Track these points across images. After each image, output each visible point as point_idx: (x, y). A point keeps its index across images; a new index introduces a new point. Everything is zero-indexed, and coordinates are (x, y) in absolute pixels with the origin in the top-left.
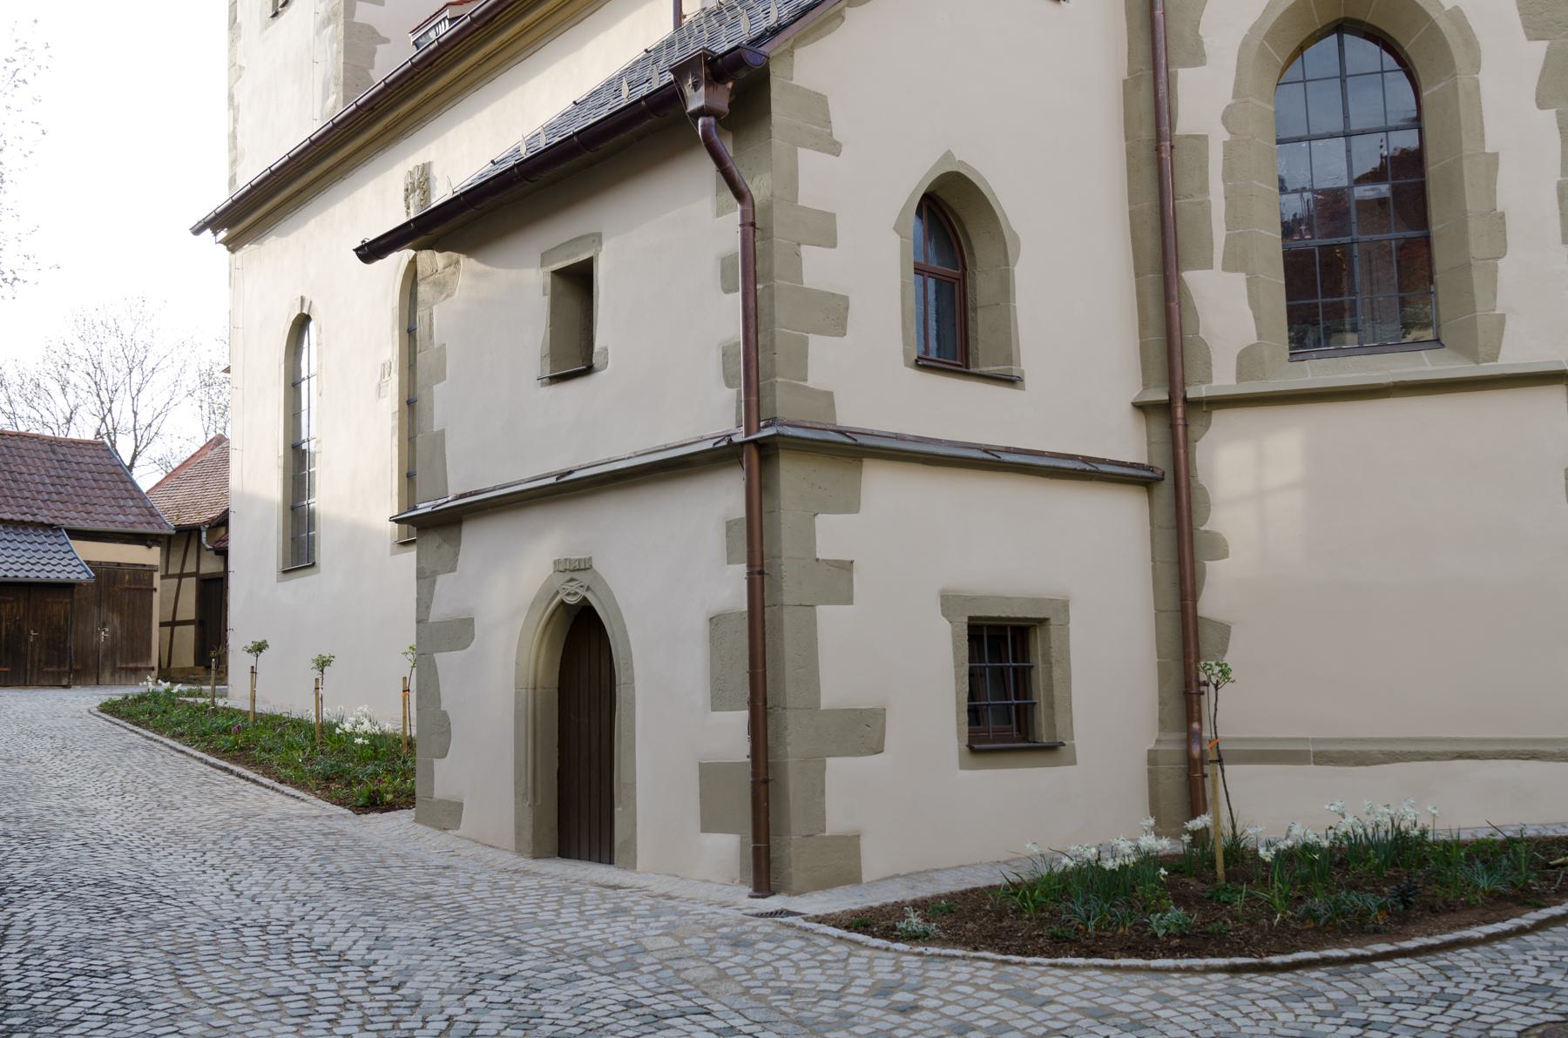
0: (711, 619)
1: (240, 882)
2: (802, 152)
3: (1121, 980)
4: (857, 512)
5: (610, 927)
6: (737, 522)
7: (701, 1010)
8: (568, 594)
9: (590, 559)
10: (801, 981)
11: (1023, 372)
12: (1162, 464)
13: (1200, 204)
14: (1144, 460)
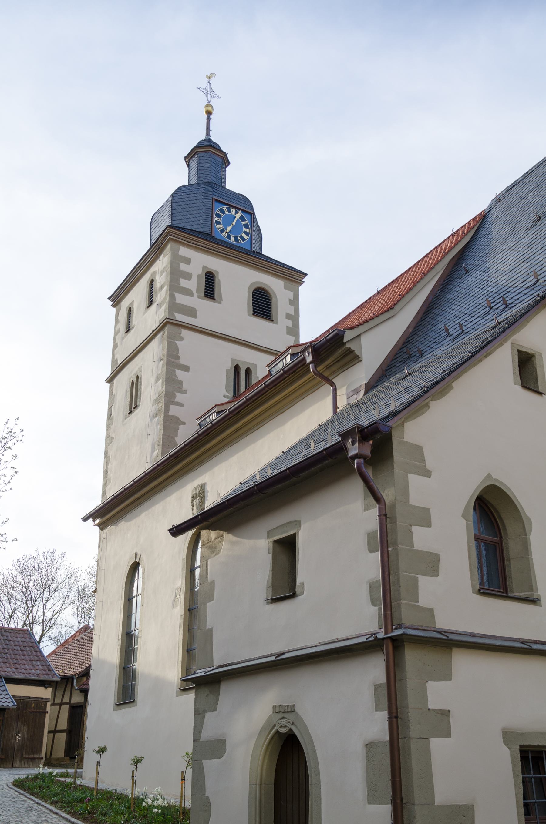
0: (366, 745)
2: (410, 476)
6: (380, 685)
8: (281, 727)
9: (294, 705)
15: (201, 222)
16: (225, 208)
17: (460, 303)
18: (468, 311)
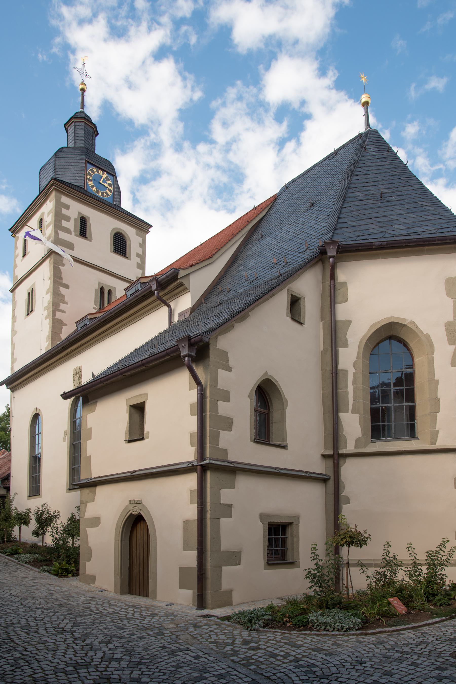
0: (184, 522)
1: (24, 602)
3: (323, 638)
4: (234, 488)
5: (152, 620)
6: (194, 491)
7: (187, 649)
8: (134, 511)
9: (142, 500)
10: (219, 639)
11: (287, 444)
12: (331, 474)
13: (345, 392)
14: (324, 473)
15: (77, 178)
16: (95, 169)
17: (256, 259)
18: (261, 264)
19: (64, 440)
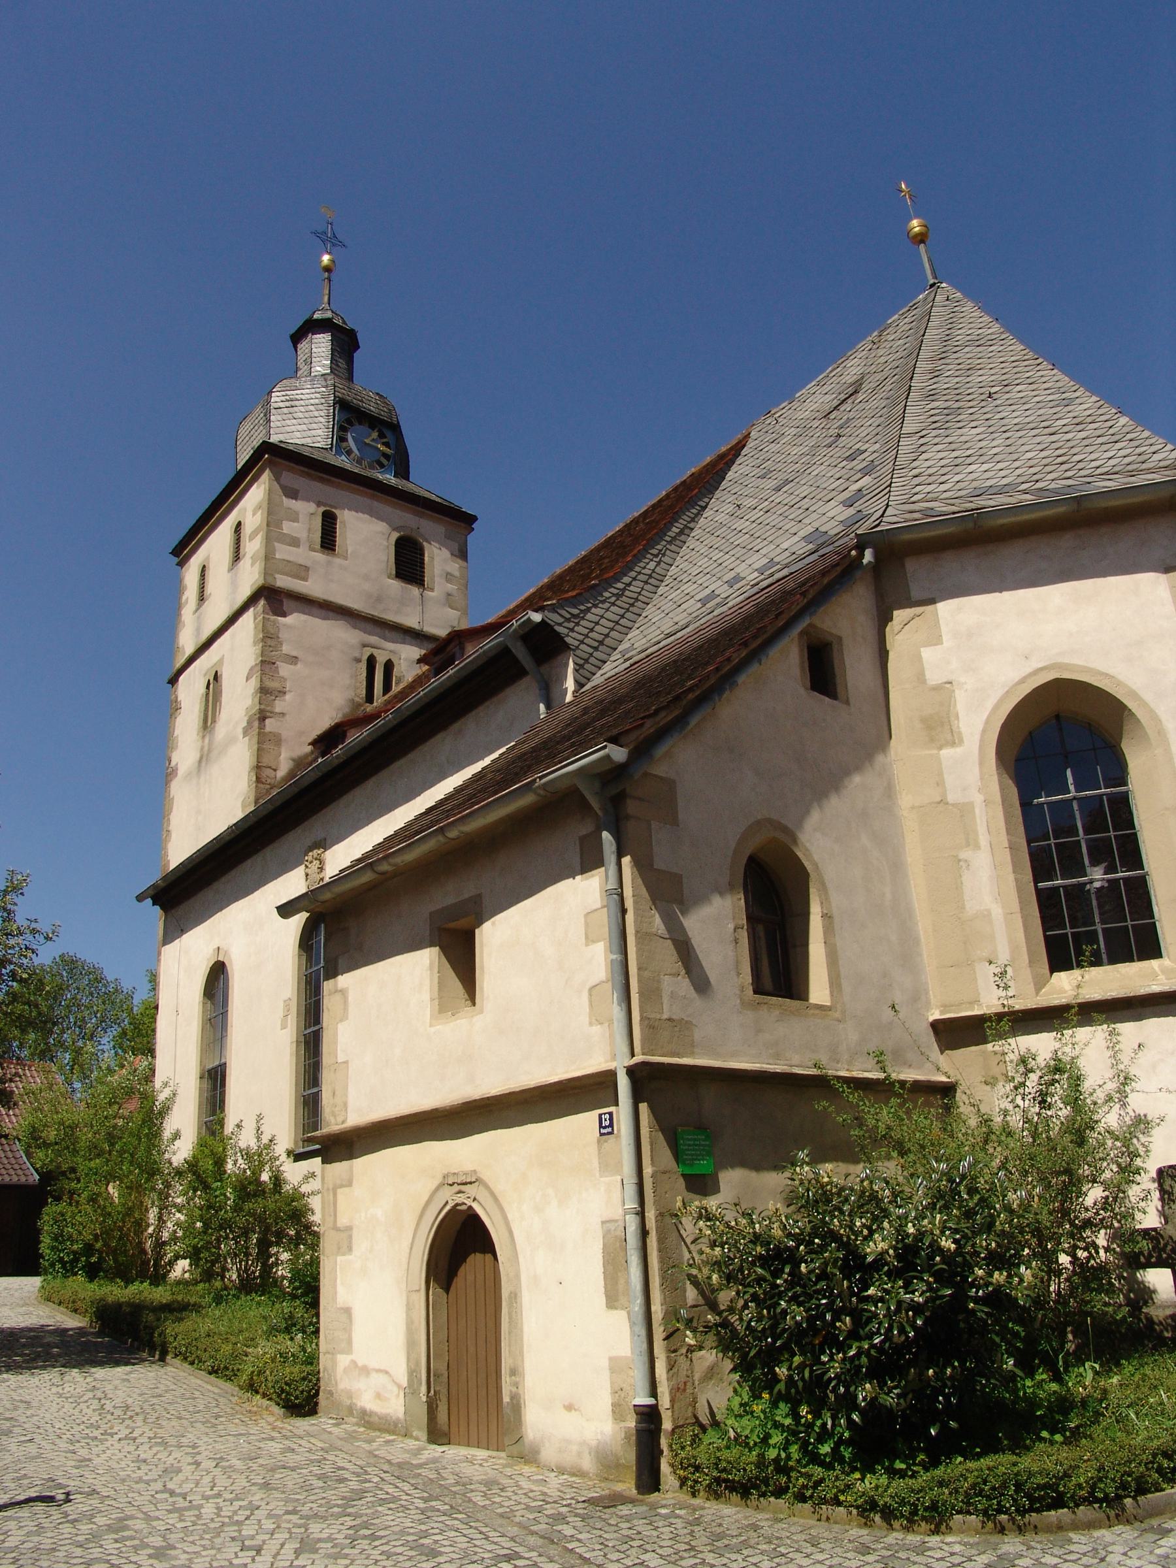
1: (171, 1479)
19: (284, 1027)
